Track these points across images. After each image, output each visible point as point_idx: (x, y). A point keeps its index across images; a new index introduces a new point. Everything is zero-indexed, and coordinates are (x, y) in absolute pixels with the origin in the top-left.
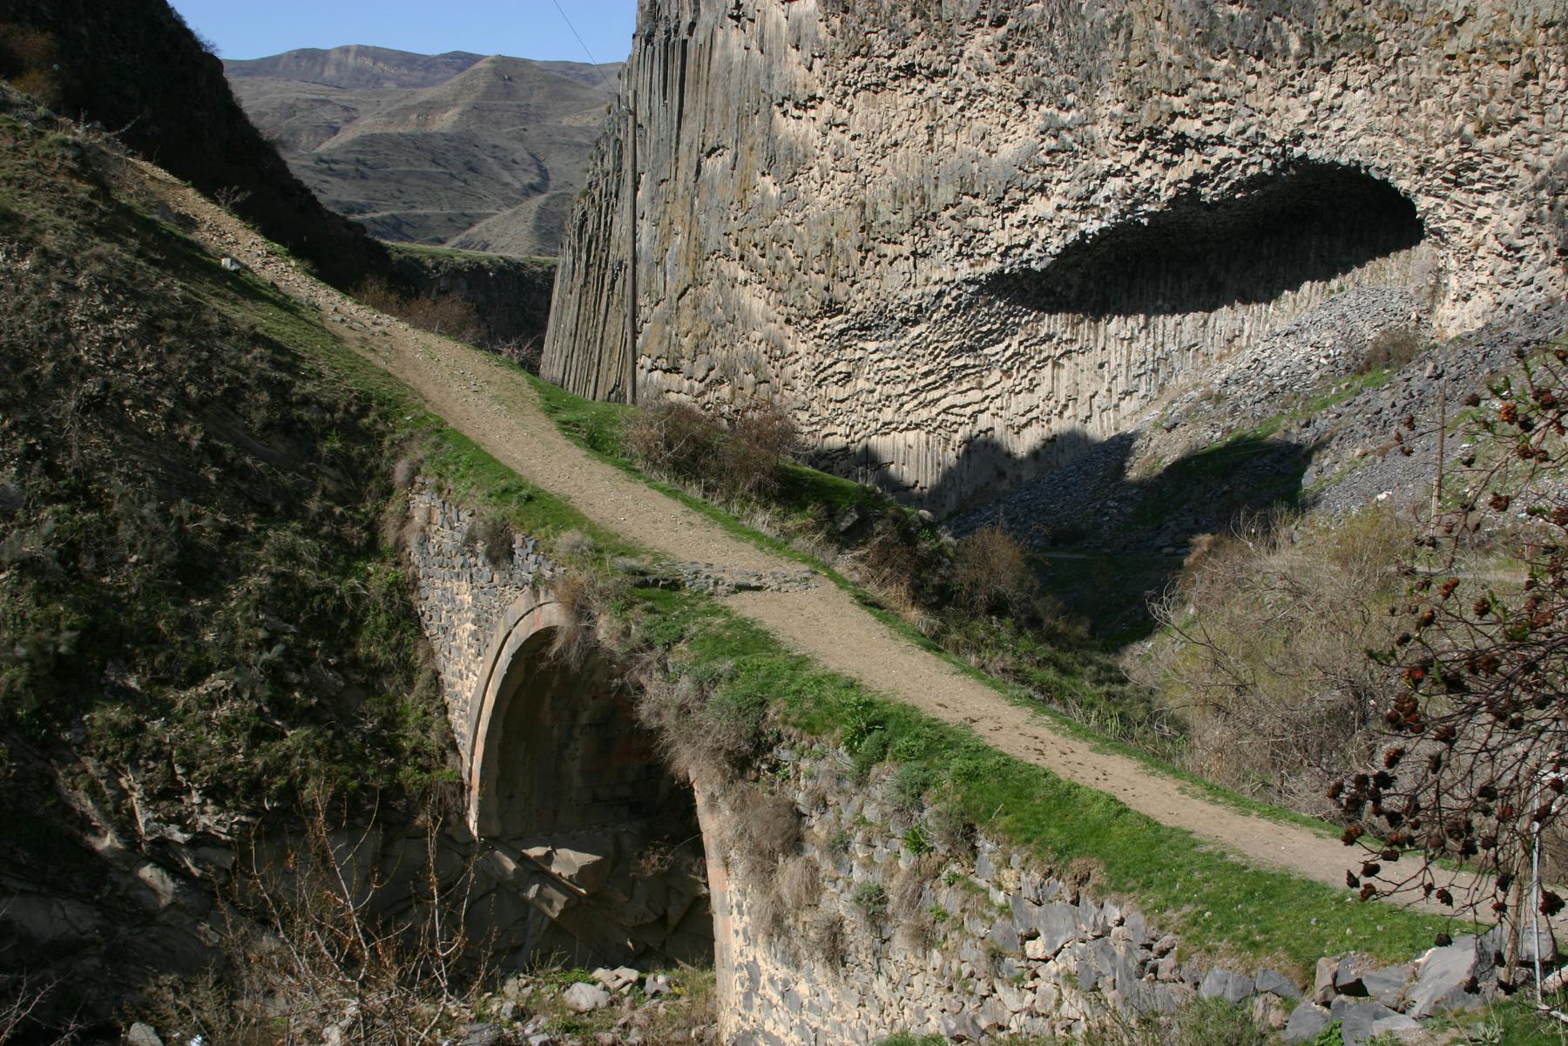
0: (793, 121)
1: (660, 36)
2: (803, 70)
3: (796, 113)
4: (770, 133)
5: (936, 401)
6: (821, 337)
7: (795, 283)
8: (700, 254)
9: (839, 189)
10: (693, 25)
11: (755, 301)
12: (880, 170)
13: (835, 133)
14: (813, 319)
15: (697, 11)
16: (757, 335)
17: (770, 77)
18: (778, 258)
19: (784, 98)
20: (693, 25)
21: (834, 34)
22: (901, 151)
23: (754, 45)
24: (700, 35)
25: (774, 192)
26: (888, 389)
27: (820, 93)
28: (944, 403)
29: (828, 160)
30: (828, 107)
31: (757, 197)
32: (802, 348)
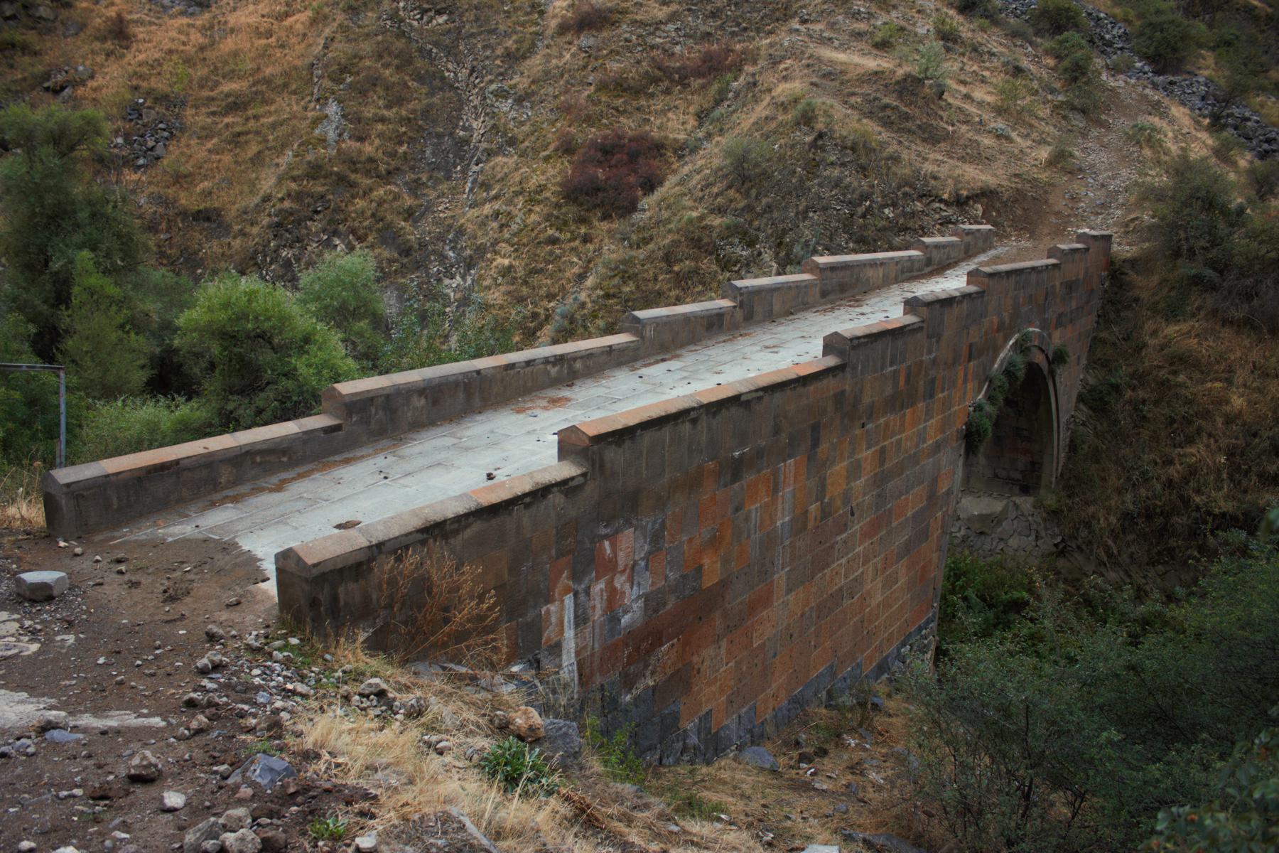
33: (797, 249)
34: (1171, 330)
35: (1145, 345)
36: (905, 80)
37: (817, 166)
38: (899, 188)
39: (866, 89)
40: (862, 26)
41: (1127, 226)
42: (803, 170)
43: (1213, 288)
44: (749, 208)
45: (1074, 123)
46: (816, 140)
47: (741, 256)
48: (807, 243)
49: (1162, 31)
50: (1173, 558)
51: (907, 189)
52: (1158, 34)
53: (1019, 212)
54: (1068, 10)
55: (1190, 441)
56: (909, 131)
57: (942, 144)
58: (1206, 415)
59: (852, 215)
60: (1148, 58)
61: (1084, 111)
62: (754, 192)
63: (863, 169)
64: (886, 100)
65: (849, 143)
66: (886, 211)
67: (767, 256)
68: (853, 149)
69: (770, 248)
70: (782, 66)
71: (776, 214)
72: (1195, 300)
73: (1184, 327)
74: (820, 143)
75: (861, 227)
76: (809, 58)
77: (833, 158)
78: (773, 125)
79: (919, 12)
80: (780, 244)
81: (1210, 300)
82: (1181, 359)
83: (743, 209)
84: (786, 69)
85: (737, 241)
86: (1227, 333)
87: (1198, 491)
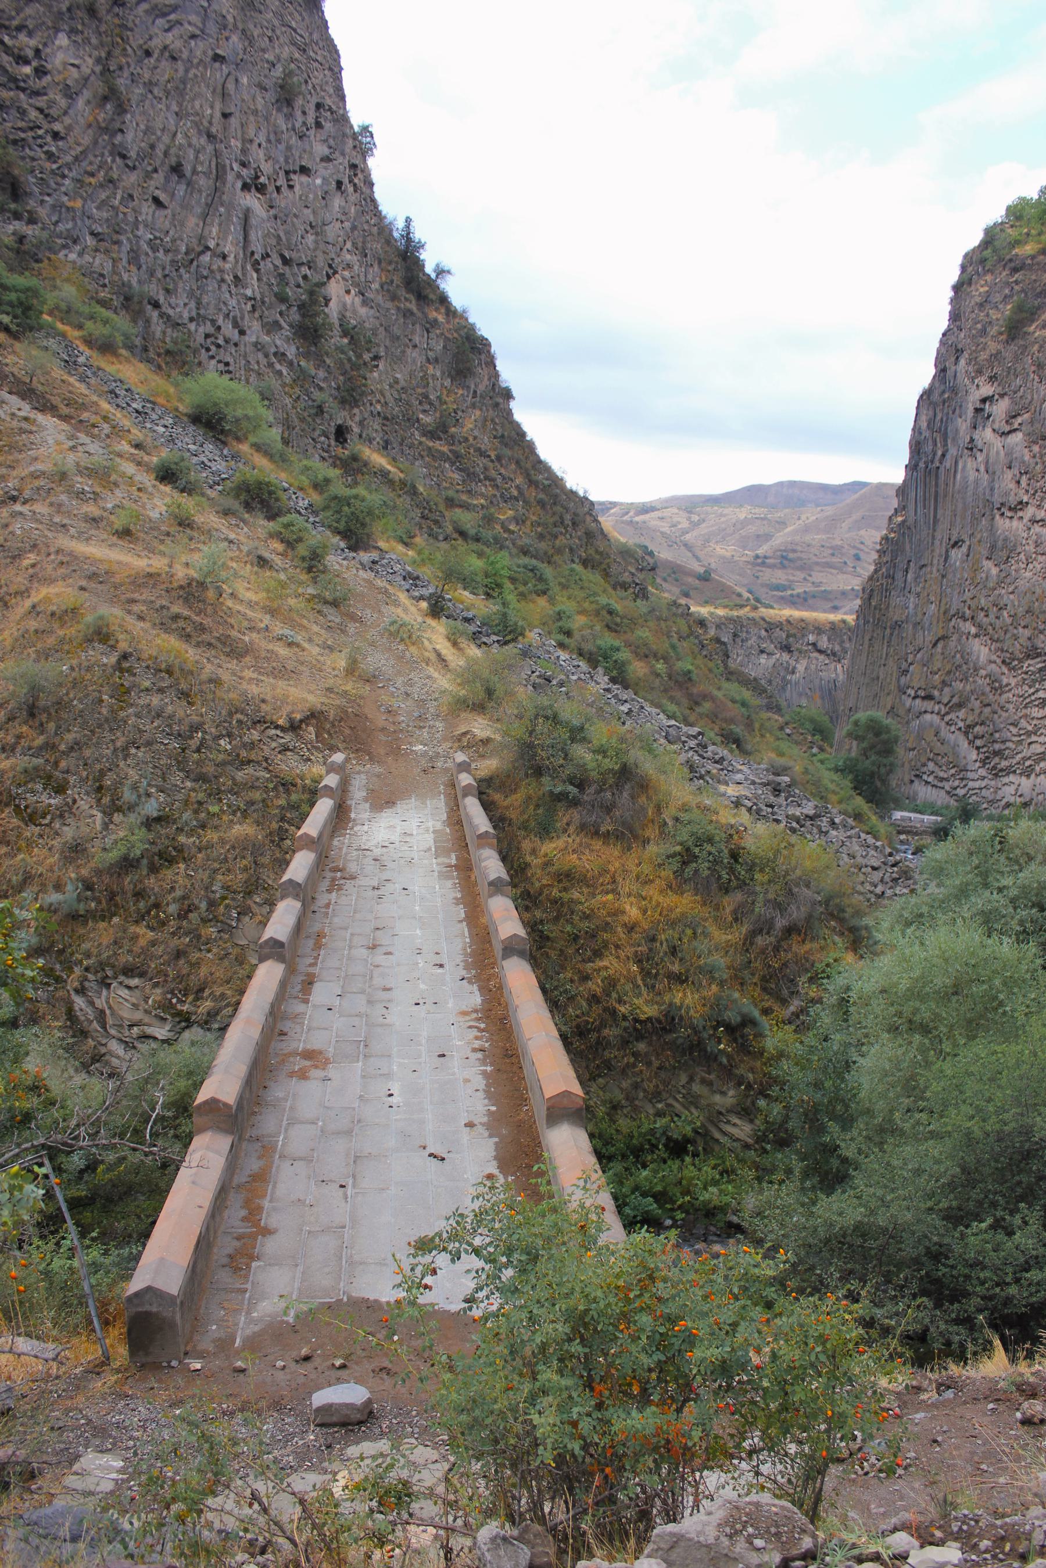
0: (1007, 521)
1: (922, 465)
2: (1012, 485)
3: (1009, 514)
4: (992, 529)
6: (1026, 673)
7: (1008, 635)
8: (947, 616)
9: (1039, 567)
10: (943, 455)
11: (981, 651)
14: (1020, 661)
15: (946, 445)
16: (983, 672)
17: (992, 489)
18: (997, 618)
19: (1002, 504)
20: (943, 455)
23: (982, 469)
24: (948, 463)
25: (994, 571)
27: (1025, 499)
29: (1031, 548)
30: (1030, 512)
31: (984, 575)
32: (1013, 682)
33: (128, 796)
34: (549, 847)
35: (527, 865)
36: (189, 584)
37: (128, 692)
38: (231, 714)
39: (146, 595)
40: (91, 509)
41: (459, 740)
42: (111, 697)
43: (575, 803)
44: (49, 746)
45: (330, 618)
46: (119, 662)
47: (50, 805)
48: (135, 787)
49: (349, 505)
50: (610, 1069)
51: (239, 716)
52: (346, 508)
53: (347, 731)
54: (268, 484)
55: (598, 954)
56: (210, 644)
57: (248, 659)
58: (607, 927)
59: (183, 750)
60: (339, 533)
61: (335, 604)
62: (51, 726)
63: (185, 695)
64: (176, 609)
65: (163, 666)
66: (222, 742)
67: (84, 804)
68: (169, 672)
69: (88, 793)
70: (26, 562)
71: (87, 753)
72: (565, 816)
73: (560, 843)
74: (126, 665)
75: (198, 763)
76: (58, 552)
77: (147, 684)
78: (51, 641)
79: (139, 490)
80: (100, 788)
81: (575, 815)
82: (568, 875)
83: (40, 748)
84: (33, 566)
85: (39, 787)
86: (597, 844)
87: (620, 1001)
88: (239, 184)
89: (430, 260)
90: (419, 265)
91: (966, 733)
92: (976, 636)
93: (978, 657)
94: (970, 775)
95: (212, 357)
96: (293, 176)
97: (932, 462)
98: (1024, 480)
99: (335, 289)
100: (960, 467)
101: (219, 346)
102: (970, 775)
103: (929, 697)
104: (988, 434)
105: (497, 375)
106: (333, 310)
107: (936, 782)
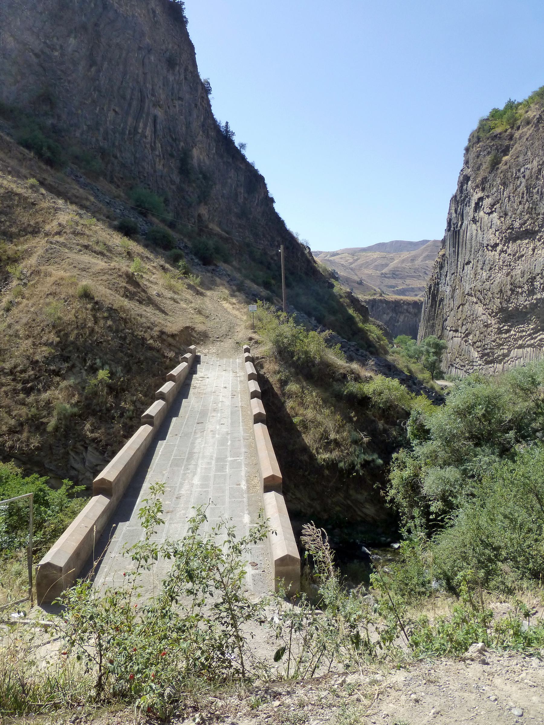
5: (536, 337)
12: (517, 265)
13: (503, 255)
15: (463, 219)
21: (502, 222)
22: (523, 258)
24: (463, 227)
26: (520, 334)
28: (539, 338)
88: (151, 105)
89: (237, 140)
90: (232, 142)
91: (473, 346)
92: (476, 303)
93: (477, 313)
94: (475, 364)
95: (142, 182)
96: (175, 101)
97: (457, 227)
98: (497, 233)
99: (195, 152)
100: (469, 228)
101: (145, 177)
102: (475, 364)
103: (456, 331)
104: (482, 213)
105: (267, 192)
106: (195, 162)
107: (460, 367)
